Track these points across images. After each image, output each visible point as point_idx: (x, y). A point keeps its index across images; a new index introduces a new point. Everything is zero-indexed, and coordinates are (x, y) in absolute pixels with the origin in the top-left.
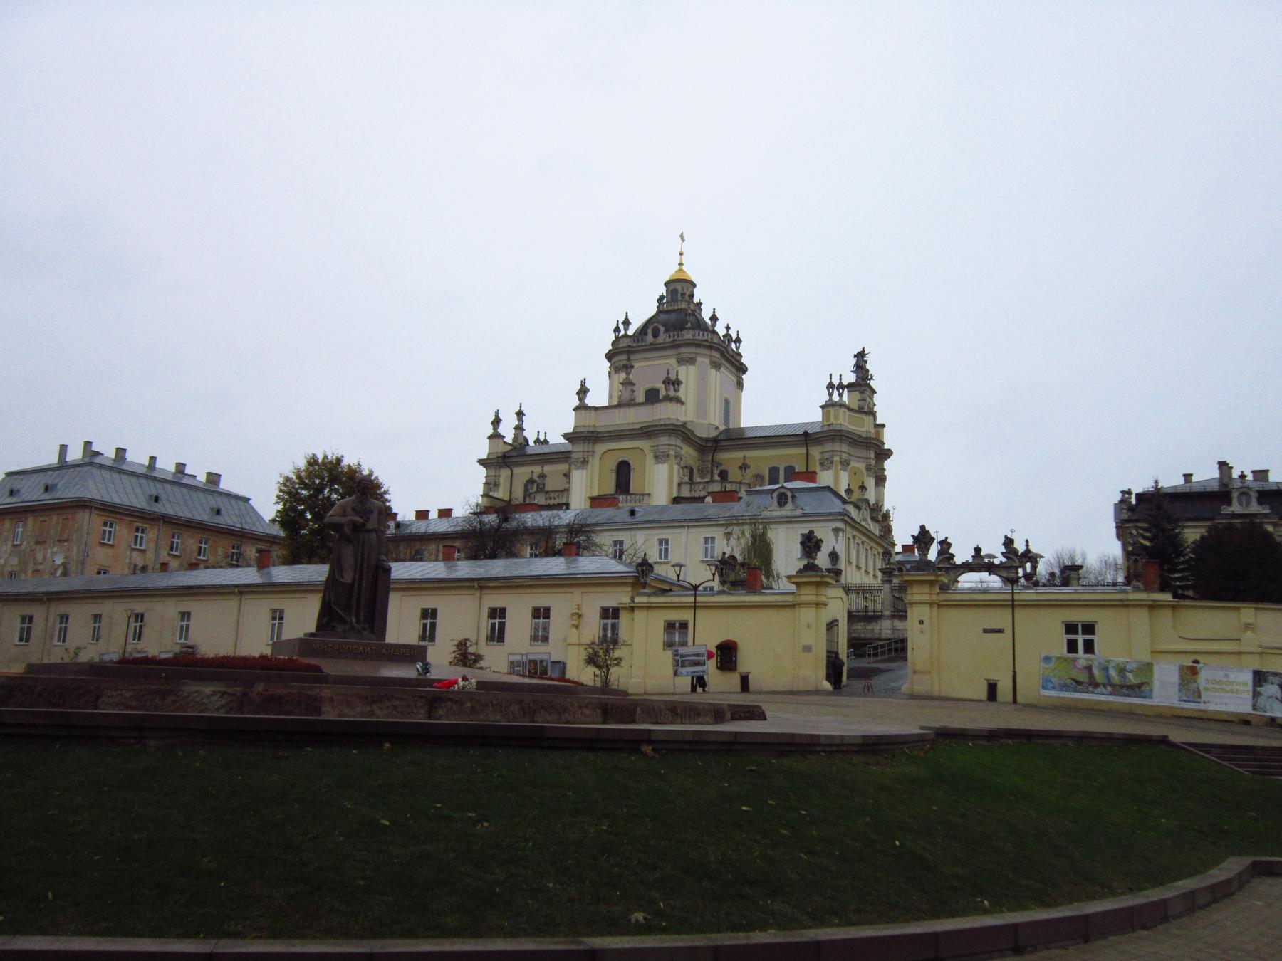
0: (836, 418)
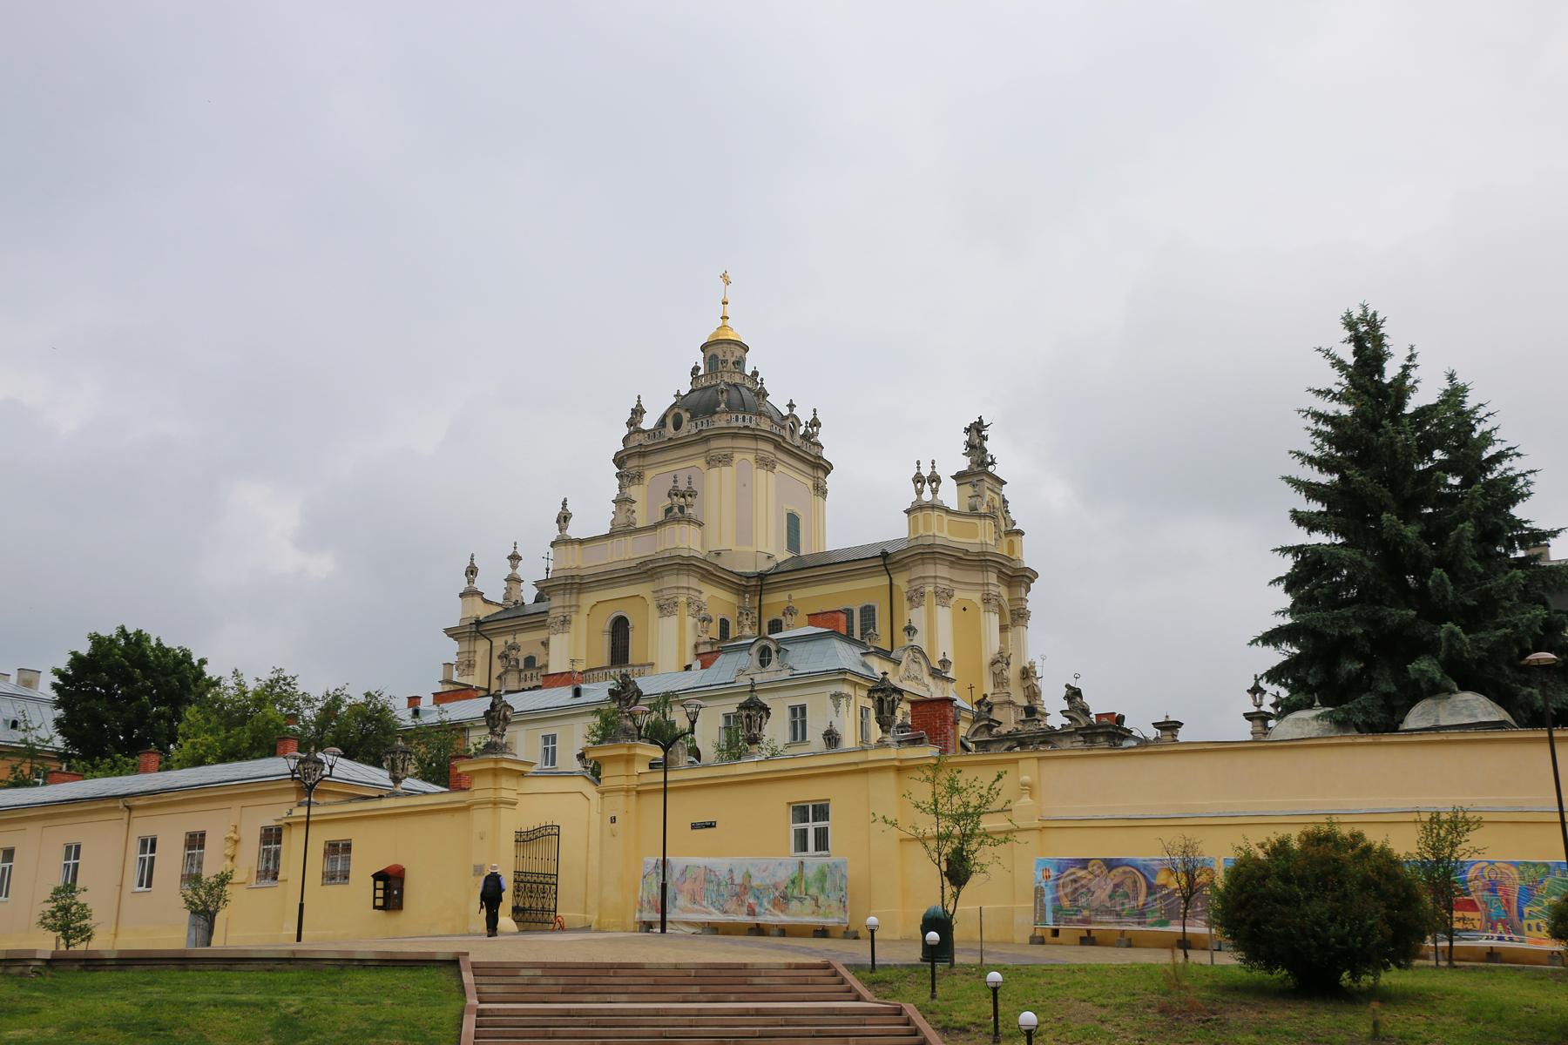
0: (927, 526)
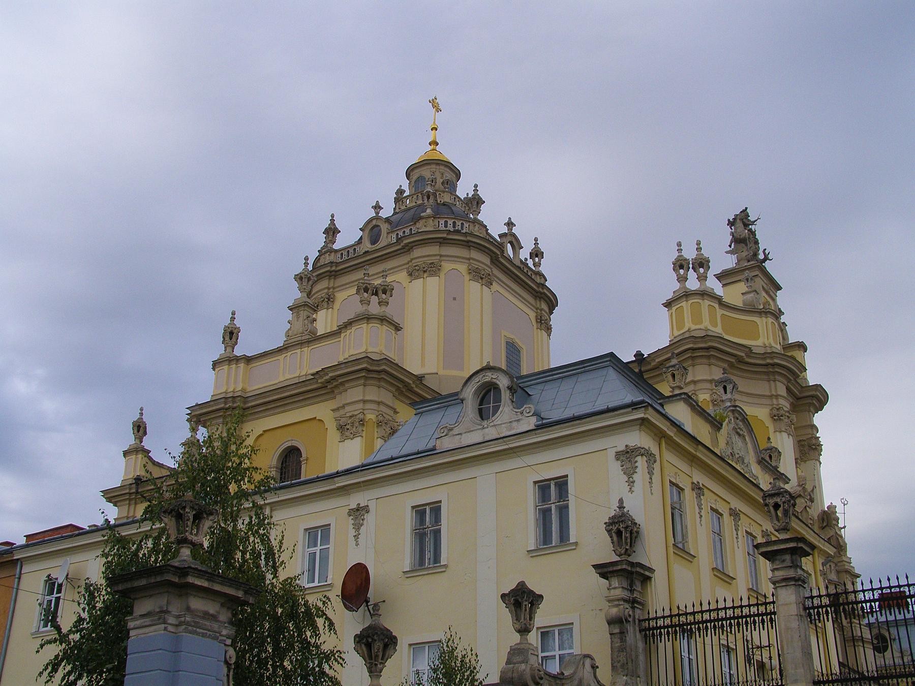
0: (697, 318)
